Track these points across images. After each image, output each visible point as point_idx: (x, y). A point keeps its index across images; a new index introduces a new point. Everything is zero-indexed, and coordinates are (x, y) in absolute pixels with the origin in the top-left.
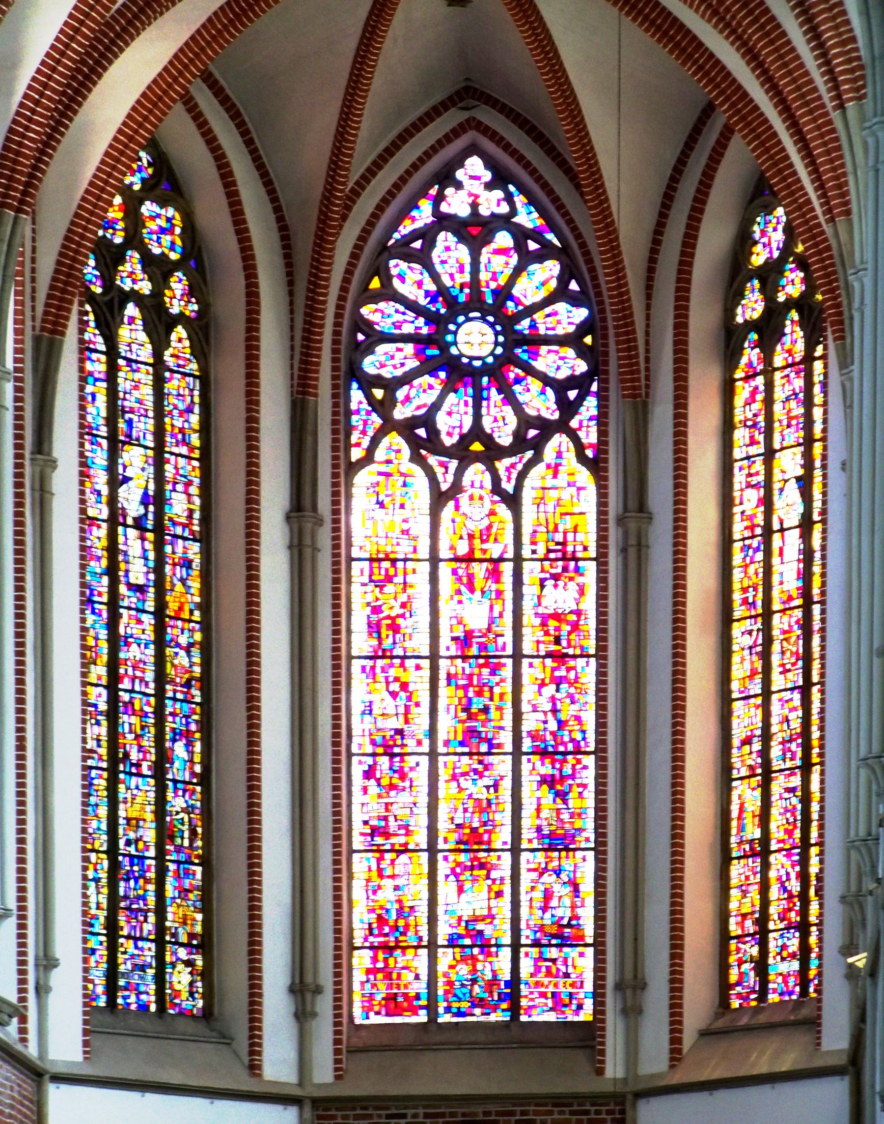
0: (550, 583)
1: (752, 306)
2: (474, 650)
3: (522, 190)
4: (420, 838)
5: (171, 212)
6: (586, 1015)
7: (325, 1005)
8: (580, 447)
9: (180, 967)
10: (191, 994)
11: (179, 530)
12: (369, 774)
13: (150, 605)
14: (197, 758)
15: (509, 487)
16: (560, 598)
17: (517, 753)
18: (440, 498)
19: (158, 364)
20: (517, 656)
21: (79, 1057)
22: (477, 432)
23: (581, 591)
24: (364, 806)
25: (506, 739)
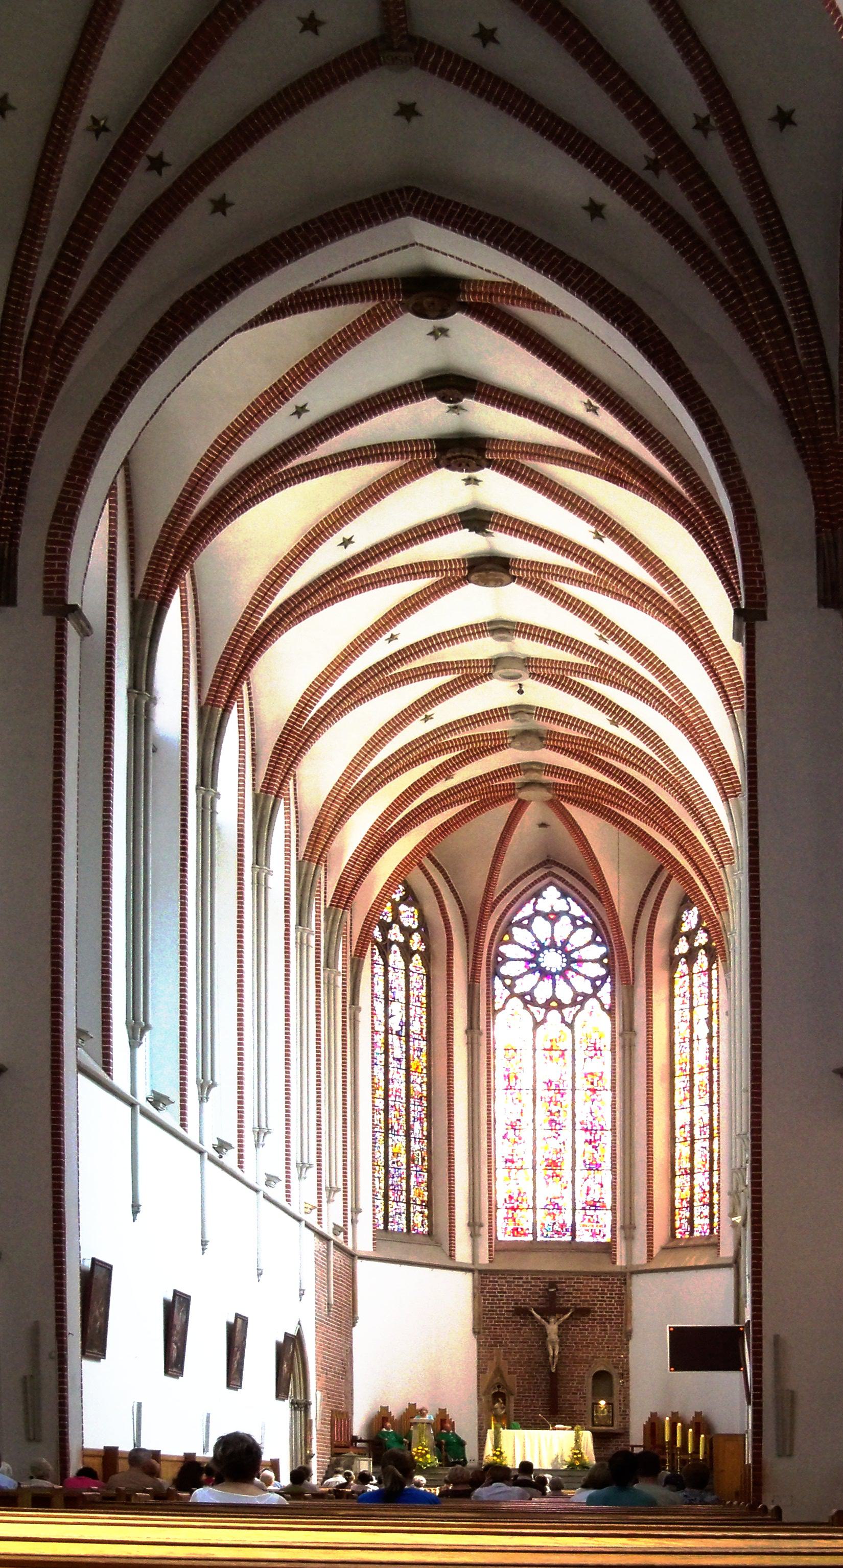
1: (682, 947)
3: (574, 900)
4: (528, 1164)
5: (413, 909)
6: (608, 1239)
8: (602, 1005)
15: (569, 1020)
17: (574, 1130)
18: (537, 1024)
19: (407, 971)
22: (553, 998)
24: (502, 1149)
25: (569, 1124)
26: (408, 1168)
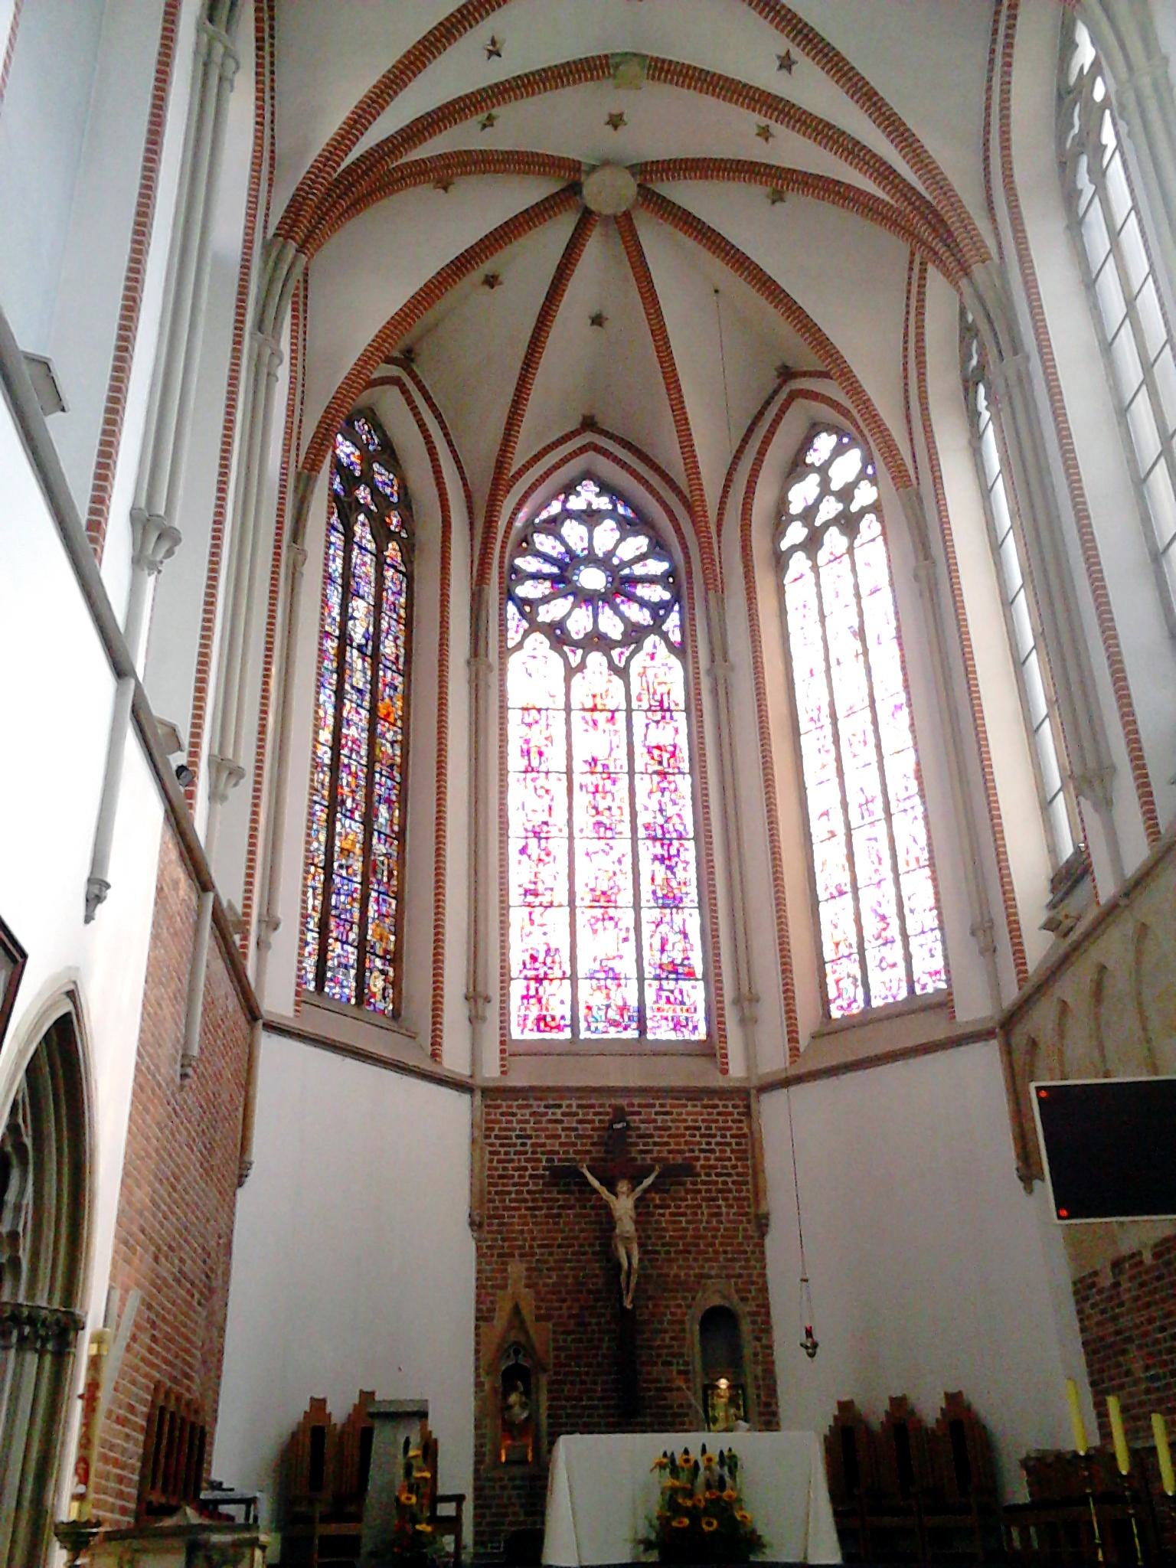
0: (653, 725)
2: (599, 768)
6: (703, 1037)
7: (492, 1012)
8: (670, 646)
9: (376, 974)
10: (384, 998)
11: (389, 664)
12: (523, 851)
13: (366, 704)
14: (396, 821)
16: (662, 735)
18: (570, 672)
20: (631, 773)
21: (291, 1014)
23: (676, 731)
24: (519, 874)
25: (625, 828)
26: (365, 882)
